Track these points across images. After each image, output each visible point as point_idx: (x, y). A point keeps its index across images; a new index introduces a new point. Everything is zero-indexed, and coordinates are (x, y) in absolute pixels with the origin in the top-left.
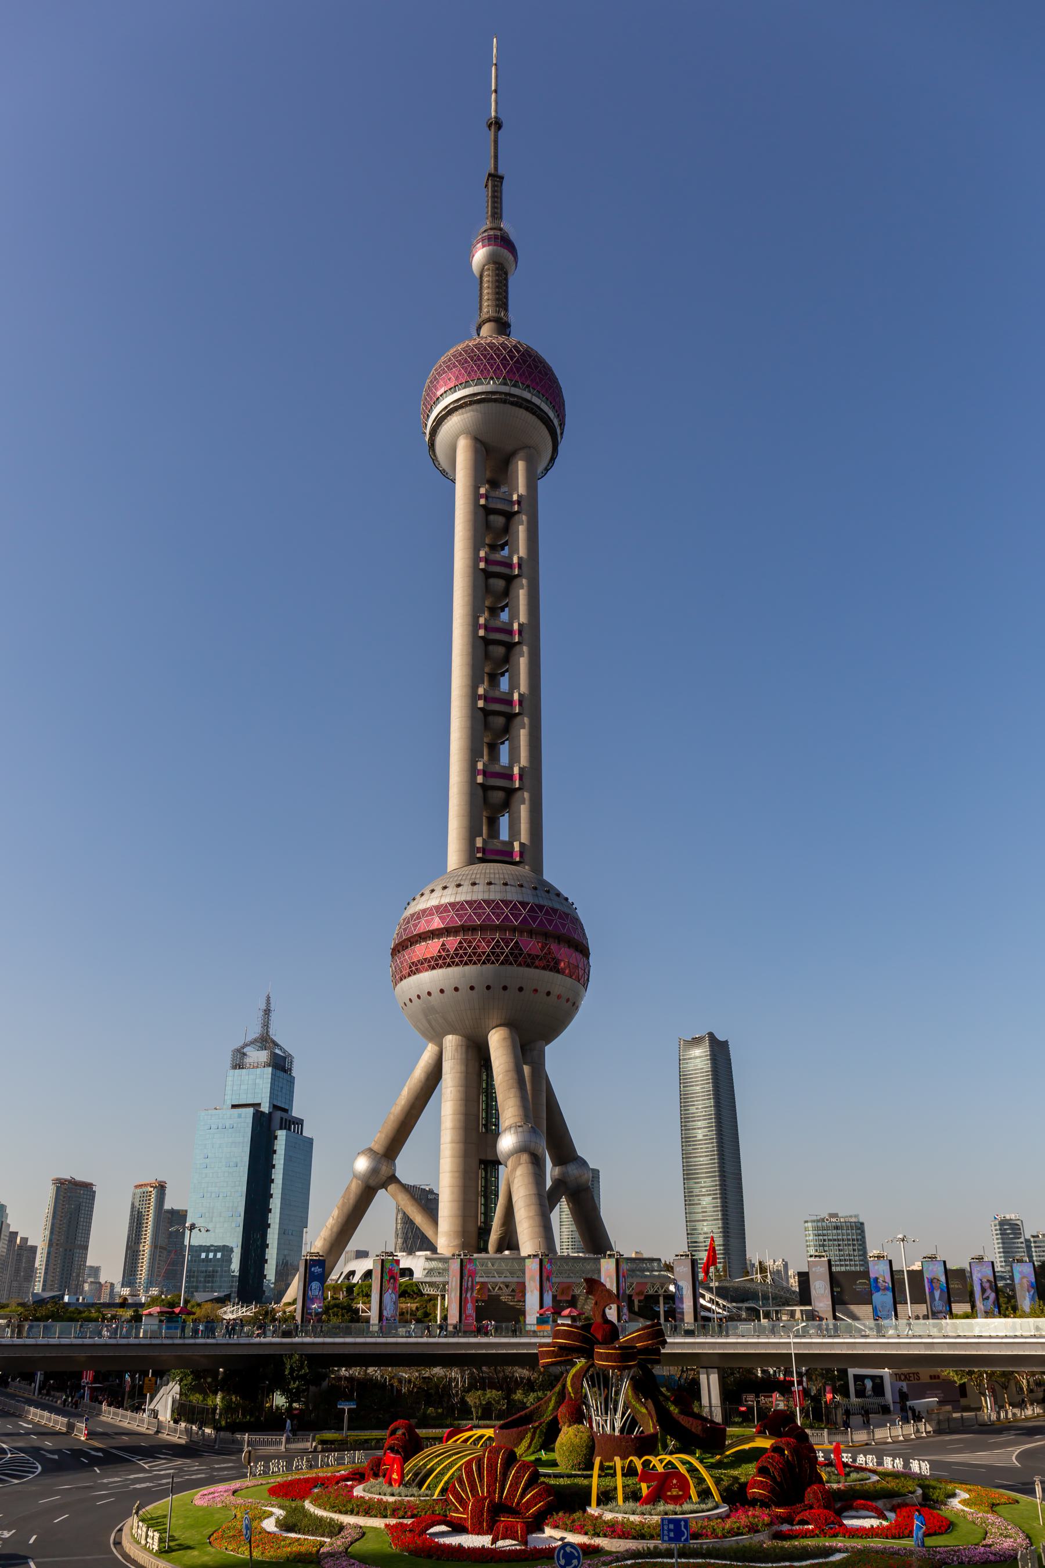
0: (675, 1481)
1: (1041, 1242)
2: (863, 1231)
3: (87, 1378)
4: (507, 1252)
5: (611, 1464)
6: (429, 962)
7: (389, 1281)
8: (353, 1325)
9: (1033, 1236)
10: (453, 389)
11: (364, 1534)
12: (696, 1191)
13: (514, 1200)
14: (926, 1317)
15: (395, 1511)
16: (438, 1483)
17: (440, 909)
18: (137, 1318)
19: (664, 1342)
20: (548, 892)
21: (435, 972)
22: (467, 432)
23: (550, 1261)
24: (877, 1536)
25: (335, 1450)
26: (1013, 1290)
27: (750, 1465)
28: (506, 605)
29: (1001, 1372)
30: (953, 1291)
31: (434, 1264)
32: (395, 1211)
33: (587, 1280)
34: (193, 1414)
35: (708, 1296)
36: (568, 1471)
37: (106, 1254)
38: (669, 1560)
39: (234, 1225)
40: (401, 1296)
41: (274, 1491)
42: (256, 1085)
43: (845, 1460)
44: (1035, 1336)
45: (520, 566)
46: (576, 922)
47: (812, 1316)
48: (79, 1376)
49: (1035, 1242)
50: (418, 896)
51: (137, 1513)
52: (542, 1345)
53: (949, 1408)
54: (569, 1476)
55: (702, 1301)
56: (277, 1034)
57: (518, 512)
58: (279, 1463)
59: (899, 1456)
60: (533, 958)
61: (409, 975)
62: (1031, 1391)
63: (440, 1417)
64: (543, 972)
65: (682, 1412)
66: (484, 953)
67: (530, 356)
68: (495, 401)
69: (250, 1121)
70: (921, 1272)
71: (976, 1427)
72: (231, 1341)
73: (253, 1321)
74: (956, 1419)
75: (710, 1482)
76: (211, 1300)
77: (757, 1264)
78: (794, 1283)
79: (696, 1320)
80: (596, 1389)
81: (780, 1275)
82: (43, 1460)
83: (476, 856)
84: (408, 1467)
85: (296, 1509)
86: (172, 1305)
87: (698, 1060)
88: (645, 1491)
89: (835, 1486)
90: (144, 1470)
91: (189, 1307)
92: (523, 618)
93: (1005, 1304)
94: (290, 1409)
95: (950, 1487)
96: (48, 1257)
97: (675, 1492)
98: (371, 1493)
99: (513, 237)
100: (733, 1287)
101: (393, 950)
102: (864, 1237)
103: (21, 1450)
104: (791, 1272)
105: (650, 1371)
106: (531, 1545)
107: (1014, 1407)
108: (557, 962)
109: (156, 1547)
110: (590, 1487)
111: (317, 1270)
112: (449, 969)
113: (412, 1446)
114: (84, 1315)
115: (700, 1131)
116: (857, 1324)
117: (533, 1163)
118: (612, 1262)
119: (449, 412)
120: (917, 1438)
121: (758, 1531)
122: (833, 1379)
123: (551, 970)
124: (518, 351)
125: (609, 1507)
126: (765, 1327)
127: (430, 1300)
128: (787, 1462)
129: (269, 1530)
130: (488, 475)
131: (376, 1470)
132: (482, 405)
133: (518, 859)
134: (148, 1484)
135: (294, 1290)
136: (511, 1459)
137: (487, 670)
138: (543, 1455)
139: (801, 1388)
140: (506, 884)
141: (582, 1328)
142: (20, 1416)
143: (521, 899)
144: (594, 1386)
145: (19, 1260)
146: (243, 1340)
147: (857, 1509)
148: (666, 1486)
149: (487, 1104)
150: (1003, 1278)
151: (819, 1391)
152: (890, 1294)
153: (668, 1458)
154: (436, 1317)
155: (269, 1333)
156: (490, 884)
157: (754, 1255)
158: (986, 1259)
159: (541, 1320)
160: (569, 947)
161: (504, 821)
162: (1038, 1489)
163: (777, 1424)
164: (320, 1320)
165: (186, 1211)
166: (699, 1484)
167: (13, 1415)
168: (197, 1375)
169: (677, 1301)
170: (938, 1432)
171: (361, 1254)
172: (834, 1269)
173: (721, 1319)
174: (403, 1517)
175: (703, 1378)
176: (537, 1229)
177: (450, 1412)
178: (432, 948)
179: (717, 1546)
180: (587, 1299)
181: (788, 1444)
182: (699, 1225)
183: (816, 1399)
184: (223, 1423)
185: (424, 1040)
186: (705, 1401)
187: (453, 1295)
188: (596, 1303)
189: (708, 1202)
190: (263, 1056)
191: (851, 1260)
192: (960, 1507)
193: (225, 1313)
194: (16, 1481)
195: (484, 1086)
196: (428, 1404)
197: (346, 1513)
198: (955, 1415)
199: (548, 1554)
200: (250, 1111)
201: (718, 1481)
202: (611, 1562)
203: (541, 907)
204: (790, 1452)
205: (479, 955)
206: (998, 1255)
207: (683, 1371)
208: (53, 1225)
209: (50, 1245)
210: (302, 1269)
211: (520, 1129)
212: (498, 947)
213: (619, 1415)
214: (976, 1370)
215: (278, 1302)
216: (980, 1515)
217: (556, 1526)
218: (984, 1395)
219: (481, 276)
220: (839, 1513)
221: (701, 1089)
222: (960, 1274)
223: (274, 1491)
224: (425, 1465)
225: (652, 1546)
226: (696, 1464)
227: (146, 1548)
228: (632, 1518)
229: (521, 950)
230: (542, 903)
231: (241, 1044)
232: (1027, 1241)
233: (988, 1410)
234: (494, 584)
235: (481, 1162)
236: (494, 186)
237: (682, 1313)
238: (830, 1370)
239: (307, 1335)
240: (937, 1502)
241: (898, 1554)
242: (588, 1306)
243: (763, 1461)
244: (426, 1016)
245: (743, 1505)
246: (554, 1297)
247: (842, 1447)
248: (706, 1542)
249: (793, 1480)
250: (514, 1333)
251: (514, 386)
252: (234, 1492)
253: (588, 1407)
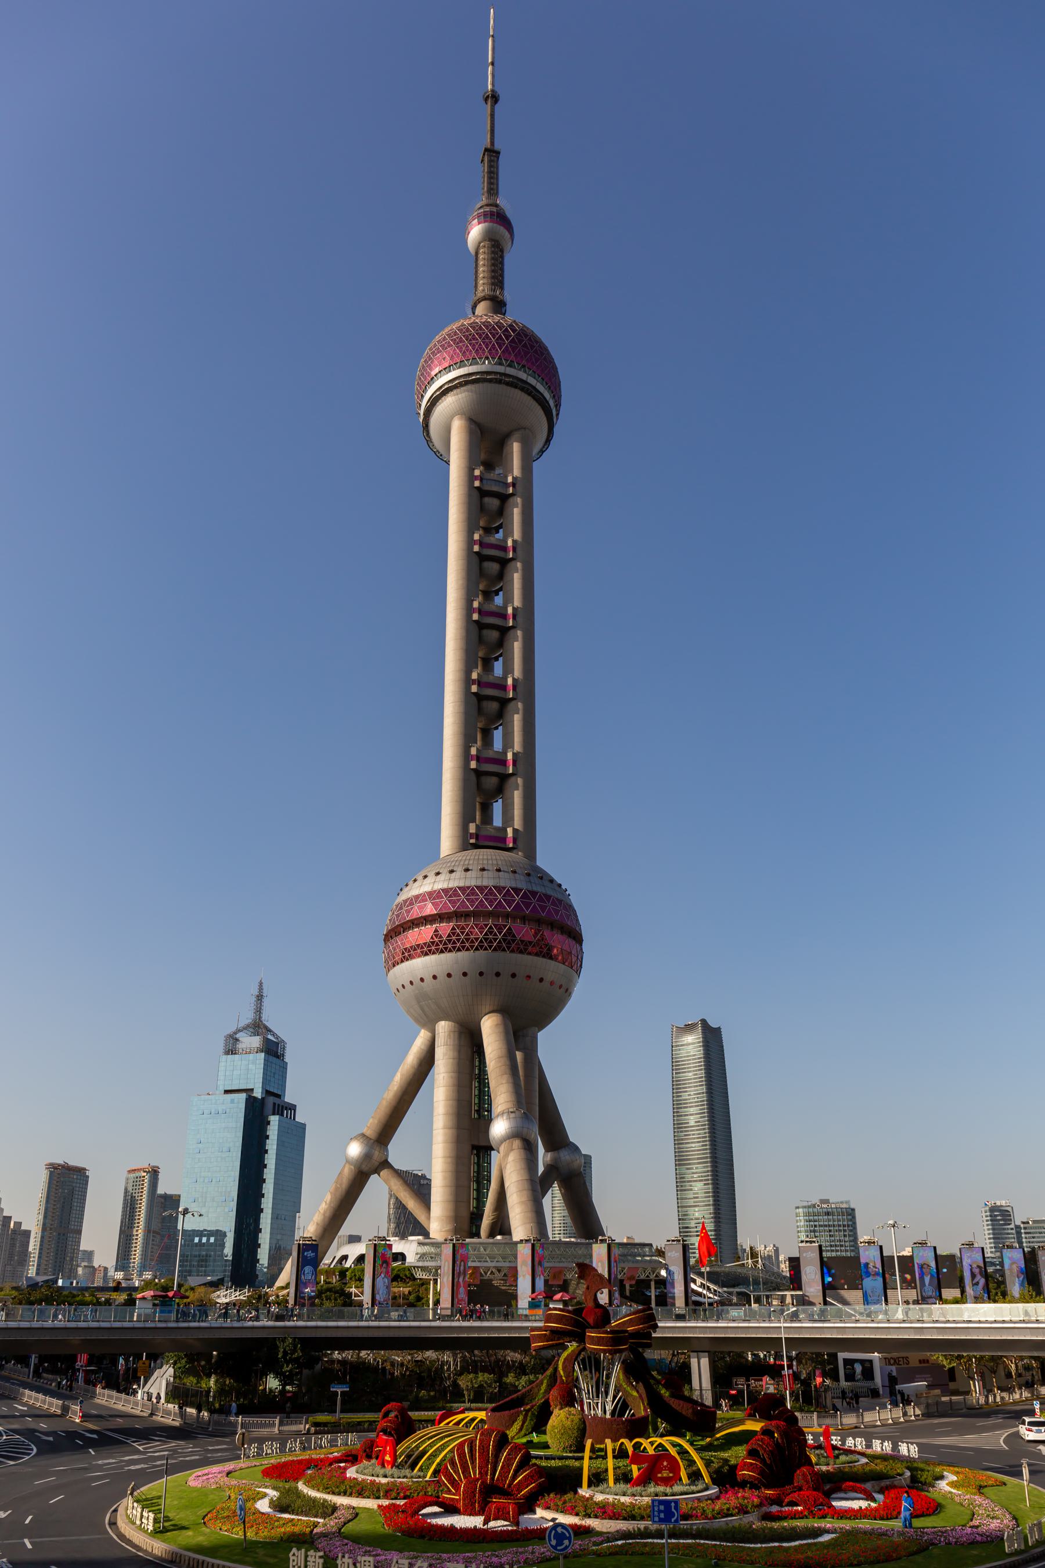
0: (665, 1463)
1: (1031, 1228)
2: (854, 1217)
3: (82, 1361)
4: (499, 1237)
5: (602, 1446)
6: (422, 948)
7: (381, 1266)
8: (346, 1309)
9: (1023, 1223)
10: (448, 369)
11: (357, 1515)
12: (688, 1177)
13: (506, 1185)
14: (916, 1302)
15: (388, 1492)
16: (431, 1464)
17: (433, 895)
18: (131, 1302)
19: (656, 1326)
20: (541, 878)
21: (427, 958)
22: (461, 413)
23: (542, 1246)
24: (865, 1517)
25: (328, 1433)
26: (1003, 1275)
27: (740, 1448)
28: (501, 589)
29: (990, 1358)
30: (943, 1276)
31: (426, 1249)
32: (388, 1196)
33: (579, 1265)
34: (187, 1397)
35: (699, 1281)
36: (559, 1454)
37: (99, 1238)
38: (659, 1541)
39: (227, 1210)
40: (393, 1280)
41: (268, 1473)
42: (249, 1070)
43: (834, 1442)
44: (1024, 1321)
45: (514, 549)
46: (570, 908)
47: (803, 1301)
48: (73, 1359)
49: (1025, 1228)
50: (411, 882)
51: (132, 1494)
52: (533, 1329)
53: (937, 1392)
54: (561, 1458)
55: (693, 1286)
56: (270, 1019)
57: (512, 495)
58: (272, 1445)
59: (888, 1439)
60: (526, 945)
61: (402, 961)
62: (1019, 1375)
63: (433, 1399)
64: (536, 958)
65: (672, 1395)
66: (476, 939)
67: (526, 336)
68: (490, 381)
69: (243, 1106)
70: (911, 1258)
71: (964, 1410)
72: (225, 1325)
73: (247, 1304)
74: (943, 1402)
75: (700, 1465)
76: (205, 1284)
77: (748, 1249)
78: (785, 1268)
79: (687, 1304)
80: (587, 1372)
81: (771, 1260)
82: (38, 1442)
83: (469, 842)
84: (400, 1449)
85: (289, 1490)
86: (166, 1288)
87: (691, 1047)
88: (635, 1473)
89: (824, 1468)
90: (138, 1452)
91: (182, 1290)
92: (517, 602)
93: (994, 1289)
94: (283, 1392)
95: (938, 1469)
96: (42, 1241)
97: (665, 1474)
98: (364, 1474)
99: (509, 214)
100: (724, 1272)
101: (386, 935)
102: (855, 1223)
103: (16, 1431)
104: (781, 1258)
105: (641, 1354)
106: (522, 1526)
107: (1002, 1389)
108: (550, 949)
109: (151, 1528)
110: (581, 1469)
111: (310, 1254)
112: (442, 955)
113: (405, 1429)
114: (78, 1299)
115: (692, 1117)
116: (847, 1309)
117: (525, 1149)
118: (604, 1248)
119: (444, 392)
120: (906, 1421)
121: (747, 1512)
122: (823, 1363)
123: (544, 956)
124: (514, 331)
125: (600, 1488)
126: (756, 1312)
127: (423, 1284)
128: (777, 1444)
129: (263, 1510)
130: (483, 456)
131: (369, 1452)
132: (477, 385)
133: (511, 845)
134: (143, 1466)
135: (287, 1274)
136: (503, 1441)
137: (481, 654)
138: (535, 1437)
139: (791, 1371)
140: (499, 870)
141: (574, 1312)
142: (14, 1399)
143: (514, 886)
144: (585, 1369)
145: (13, 1245)
146: (236, 1324)
147: (845, 1491)
148: (656, 1469)
149: (480, 1090)
150: (993, 1264)
151: (809, 1374)
152: (880, 1279)
153: (659, 1440)
154: (428, 1301)
155: (262, 1317)
156: (483, 870)
157: (744, 1241)
158: (976, 1245)
159: (533, 1305)
160: (562, 933)
161: (497, 807)
162: (1025, 1472)
163: (766, 1407)
164: (313, 1304)
165: (179, 1196)
166: (689, 1466)
167: (8, 1398)
168: (191, 1358)
169: (668, 1285)
170: (927, 1415)
171: (354, 1239)
172: (824, 1254)
173: (711, 1304)
174: (396, 1498)
175: (694, 1362)
176: (529, 1215)
177: (443, 1395)
178: (424, 934)
179: (707, 1526)
180: (578, 1283)
181: (778, 1427)
182: (691, 1211)
183: (806, 1383)
184: (217, 1405)
185: (418, 1027)
186: (695, 1384)
187: (445, 1280)
188: (588, 1288)
189: (700, 1188)
190: (256, 1041)
191: (841, 1246)
192: (948, 1489)
193: (219, 1296)
194: (12, 1463)
195: (477, 1072)
196: (421, 1387)
197: (339, 1494)
198: (944, 1399)
199: (539, 1535)
200: (244, 1096)
201: (708, 1464)
202: (602, 1543)
203: (534, 894)
204: (780, 1434)
205: (472, 942)
206: (988, 1241)
207: (673, 1355)
208: (46, 1209)
209: (44, 1229)
210: (295, 1253)
211: (512, 1115)
212: (491, 933)
213: (610, 1398)
214: (965, 1354)
215: (271, 1286)
216: (968, 1497)
217: (547, 1508)
218: (973, 1379)
219: (477, 253)
220: (828, 1495)
221: (694, 1076)
222: (952, 1257)
223: (268, 1473)
224: (417, 1447)
225: (642, 1527)
226: (687, 1446)
227: (141, 1529)
228: (623, 1499)
229: (514, 936)
230: (535, 889)
231: (234, 1029)
232: (1017, 1227)
233: (977, 1393)
234: (488, 567)
235: (474, 1147)
236: (490, 161)
237: (674, 1298)
238: (820, 1355)
239: (300, 1317)
240: (925, 1484)
241: (886, 1535)
242: (579, 1291)
243: (753, 1444)
244: (419, 1002)
245: (733, 1486)
246: (546, 1282)
247: (831, 1430)
248: (696, 1523)
249: (783, 1462)
250: (506, 1317)
251: (510, 366)
252: (228, 1473)
253: (579, 1390)
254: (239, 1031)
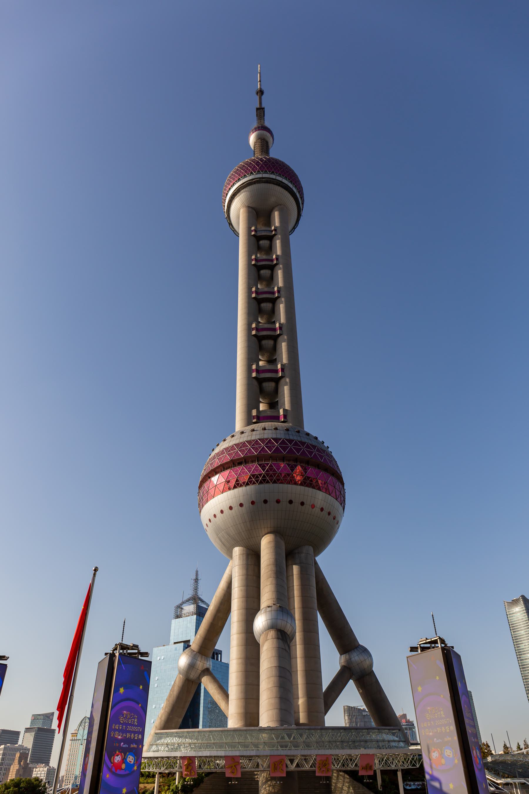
20: (298, 432)
83: (249, 420)
231: (180, 602)
254: (183, 603)
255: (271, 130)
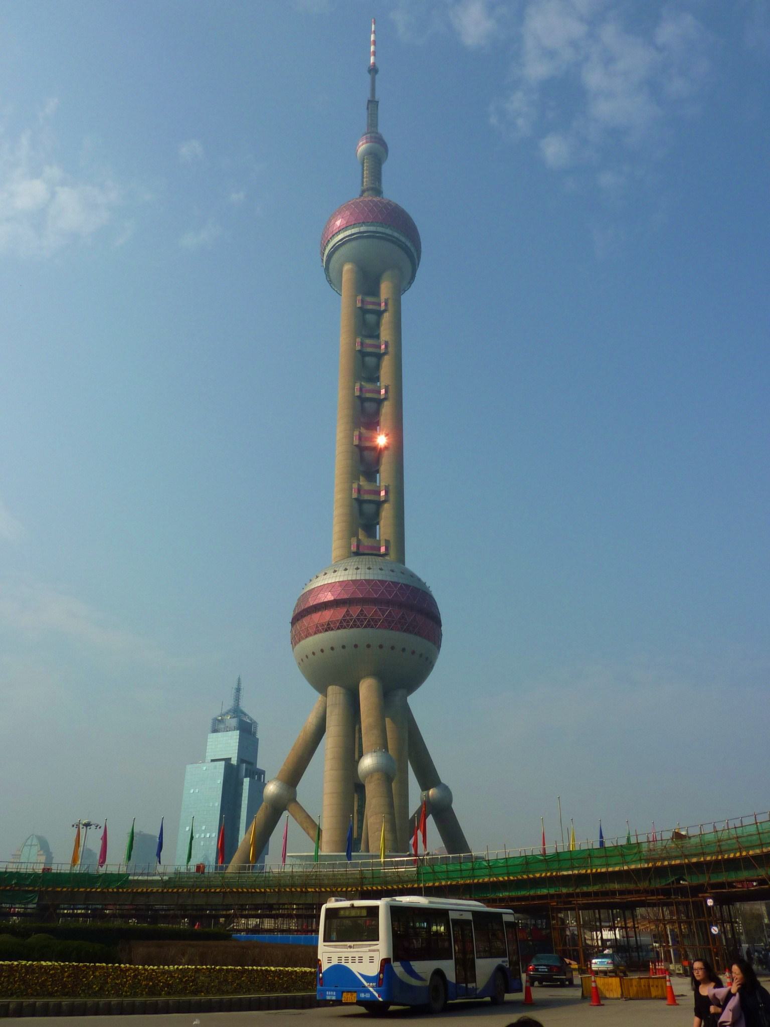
56: (245, 706)
69: (222, 771)
119: (336, 248)
255: (389, 146)
